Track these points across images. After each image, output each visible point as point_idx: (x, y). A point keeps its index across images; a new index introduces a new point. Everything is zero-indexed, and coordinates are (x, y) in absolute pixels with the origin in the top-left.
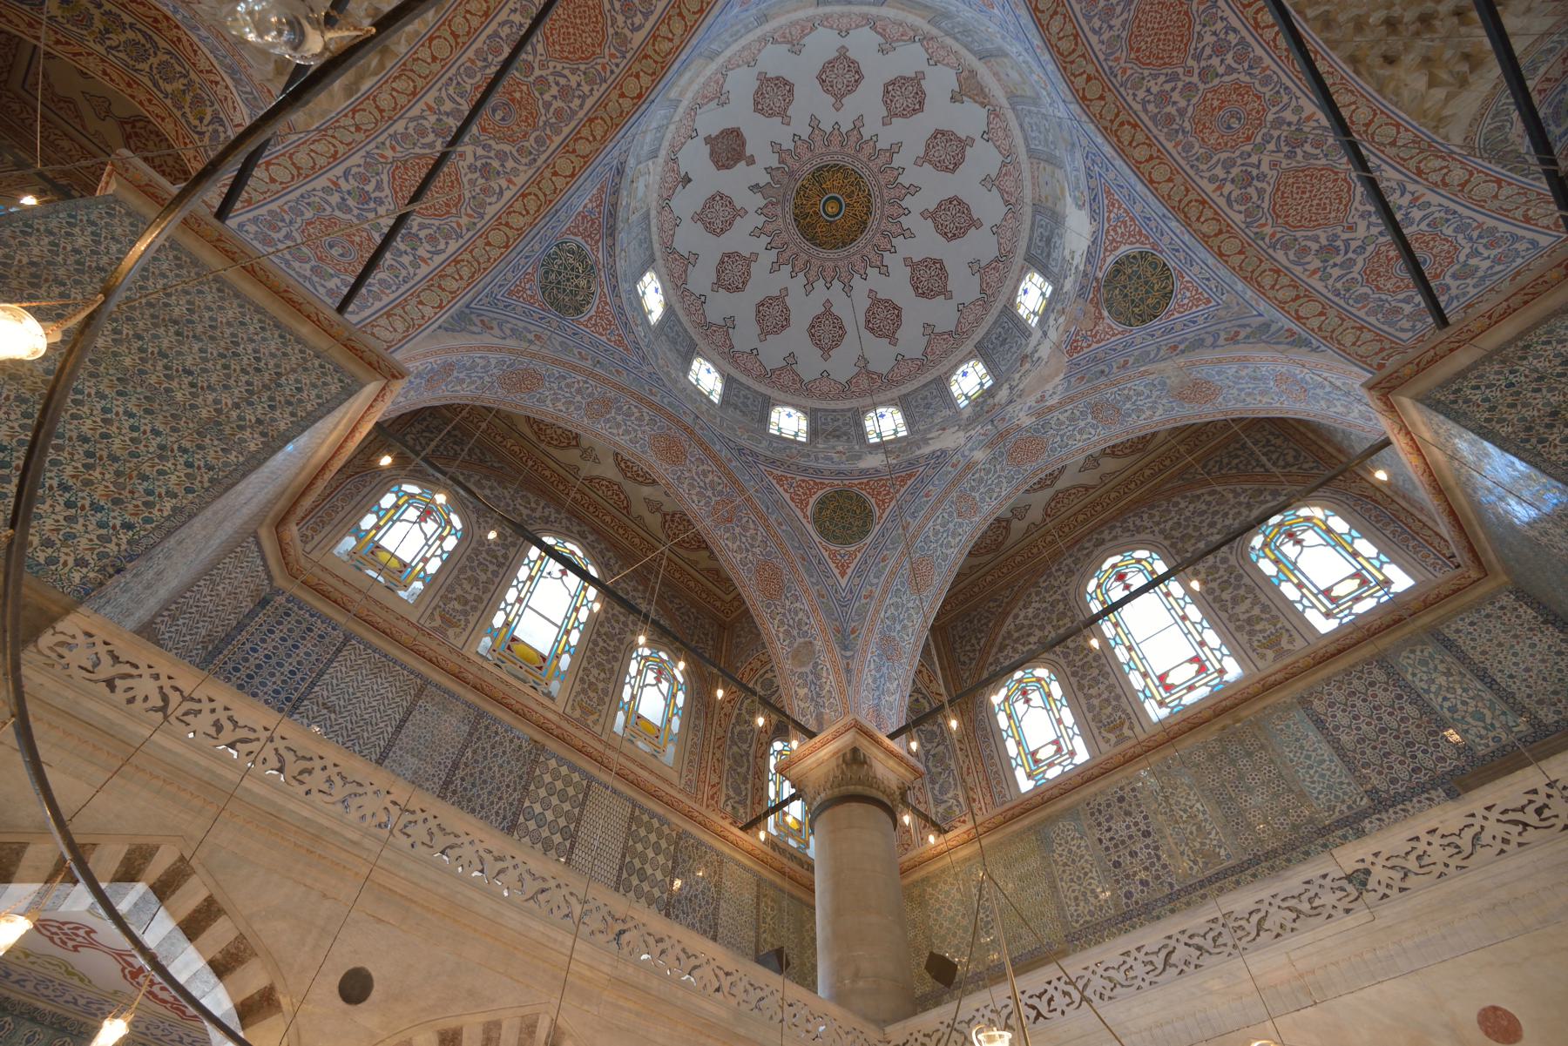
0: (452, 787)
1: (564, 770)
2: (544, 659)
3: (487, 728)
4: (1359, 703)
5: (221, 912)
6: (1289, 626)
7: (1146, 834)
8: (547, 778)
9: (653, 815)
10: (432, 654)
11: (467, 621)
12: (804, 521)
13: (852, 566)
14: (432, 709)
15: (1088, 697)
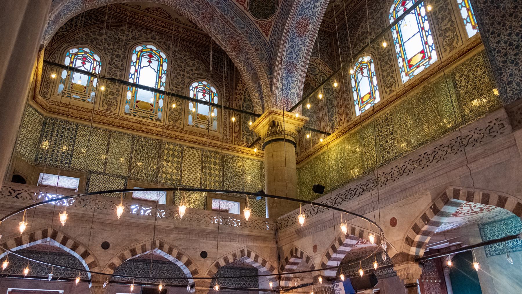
0: (132, 165)
1: (171, 147)
2: (152, 105)
3: (138, 141)
4: (471, 75)
5: (68, 239)
6: (458, 35)
7: (392, 133)
8: (166, 152)
9: (211, 152)
10: (108, 122)
11: (117, 102)
12: (245, 11)
13: (271, 29)
14: (116, 141)
15: (383, 71)
